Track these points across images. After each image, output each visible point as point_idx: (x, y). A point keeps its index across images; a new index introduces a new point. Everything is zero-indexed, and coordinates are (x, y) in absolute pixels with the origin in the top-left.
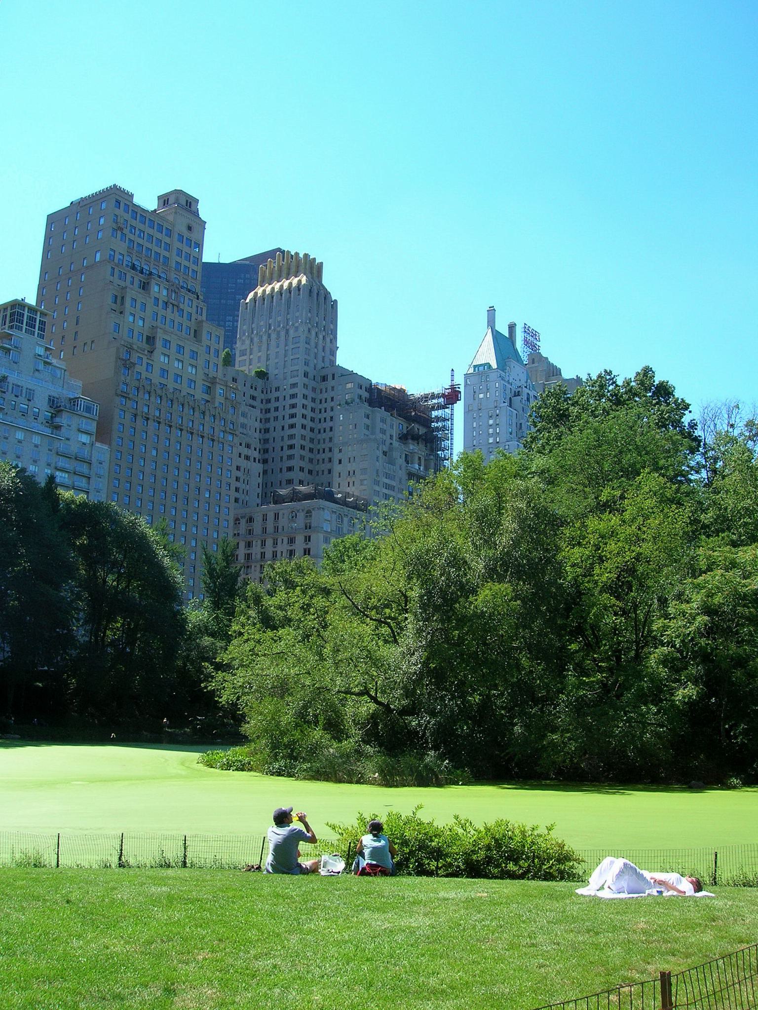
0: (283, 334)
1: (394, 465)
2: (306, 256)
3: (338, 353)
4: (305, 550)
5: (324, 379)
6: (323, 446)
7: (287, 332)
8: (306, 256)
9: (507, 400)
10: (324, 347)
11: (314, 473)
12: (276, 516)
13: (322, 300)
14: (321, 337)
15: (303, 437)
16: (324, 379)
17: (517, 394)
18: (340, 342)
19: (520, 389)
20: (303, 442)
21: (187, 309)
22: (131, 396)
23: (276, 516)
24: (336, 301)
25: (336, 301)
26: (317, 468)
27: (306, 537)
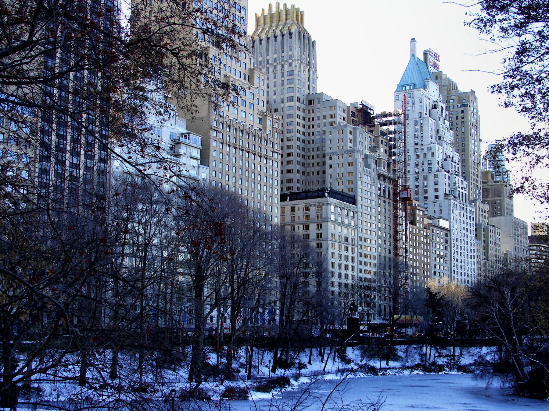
0: (279, 68)
1: (369, 168)
2: (293, 6)
3: (318, 81)
4: (317, 235)
5: (311, 102)
6: (313, 153)
7: (283, 66)
8: (293, 6)
9: (428, 113)
10: (309, 78)
11: (306, 174)
12: (293, 209)
13: (307, 41)
14: (307, 70)
15: (298, 147)
16: (311, 102)
17: (435, 107)
18: (318, 74)
19: (436, 103)
20: (299, 151)
21: (243, 60)
22: (219, 130)
23: (293, 209)
24: (315, 41)
25: (314, 43)
26: (308, 170)
27: (318, 225)
